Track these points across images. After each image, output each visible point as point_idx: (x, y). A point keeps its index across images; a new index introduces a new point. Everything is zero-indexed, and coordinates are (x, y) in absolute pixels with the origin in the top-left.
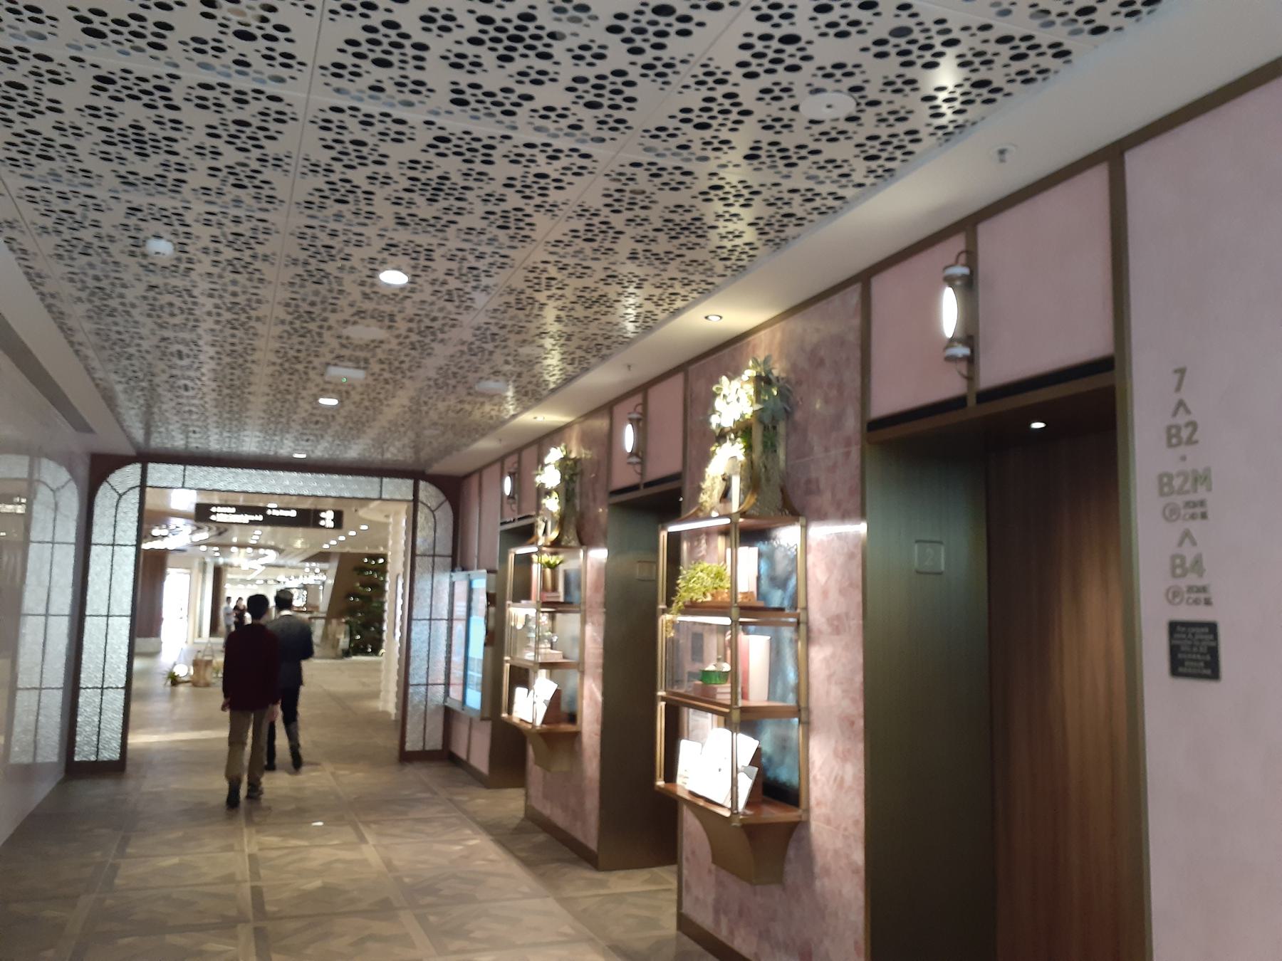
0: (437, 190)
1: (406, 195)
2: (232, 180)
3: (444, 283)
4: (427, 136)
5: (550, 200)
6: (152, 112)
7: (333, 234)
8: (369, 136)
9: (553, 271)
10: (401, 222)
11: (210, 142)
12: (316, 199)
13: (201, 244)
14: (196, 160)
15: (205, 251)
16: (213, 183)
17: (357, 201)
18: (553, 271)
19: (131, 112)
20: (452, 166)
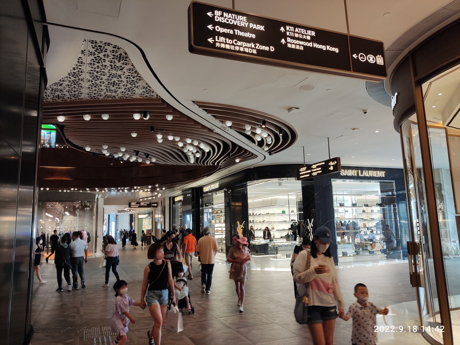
11: (69, 76)
12: (90, 87)
13: (67, 97)
16: (70, 84)
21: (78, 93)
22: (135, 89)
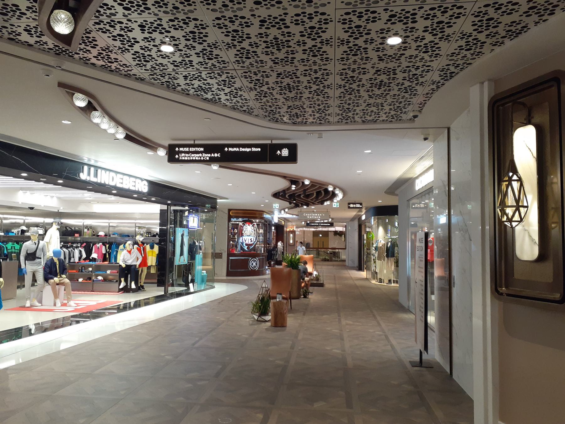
0: (381, 85)
1: (371, 89)
2: (316, 94)
3: (389, 113)
4: (373, 71)
5: (420, 81)
6: (292, 80)
7: (349, 104)
8: (355, 74)
10: (370, 97)
13: (309, 114)
14: (305, 90)
15: (311, 115)
16: (311, 96)
17: (355, 93)
19: (287, 81)
20: (384, 77)
21: (325, 107)
22: (417, 87)
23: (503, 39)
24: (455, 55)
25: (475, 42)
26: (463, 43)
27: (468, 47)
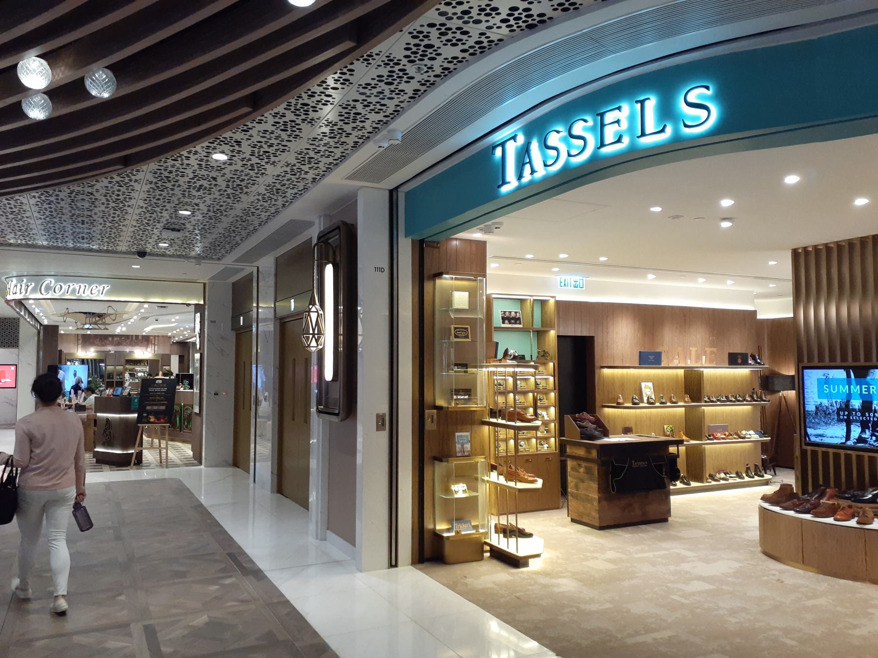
3: (250, 160)
5: (310, 117)
9: (312, 154)
18: (312, 154)
23: (436, 79)
24: (369, 87)
25: (401, 74)
26: (384, 71)
27: (390, 80)
